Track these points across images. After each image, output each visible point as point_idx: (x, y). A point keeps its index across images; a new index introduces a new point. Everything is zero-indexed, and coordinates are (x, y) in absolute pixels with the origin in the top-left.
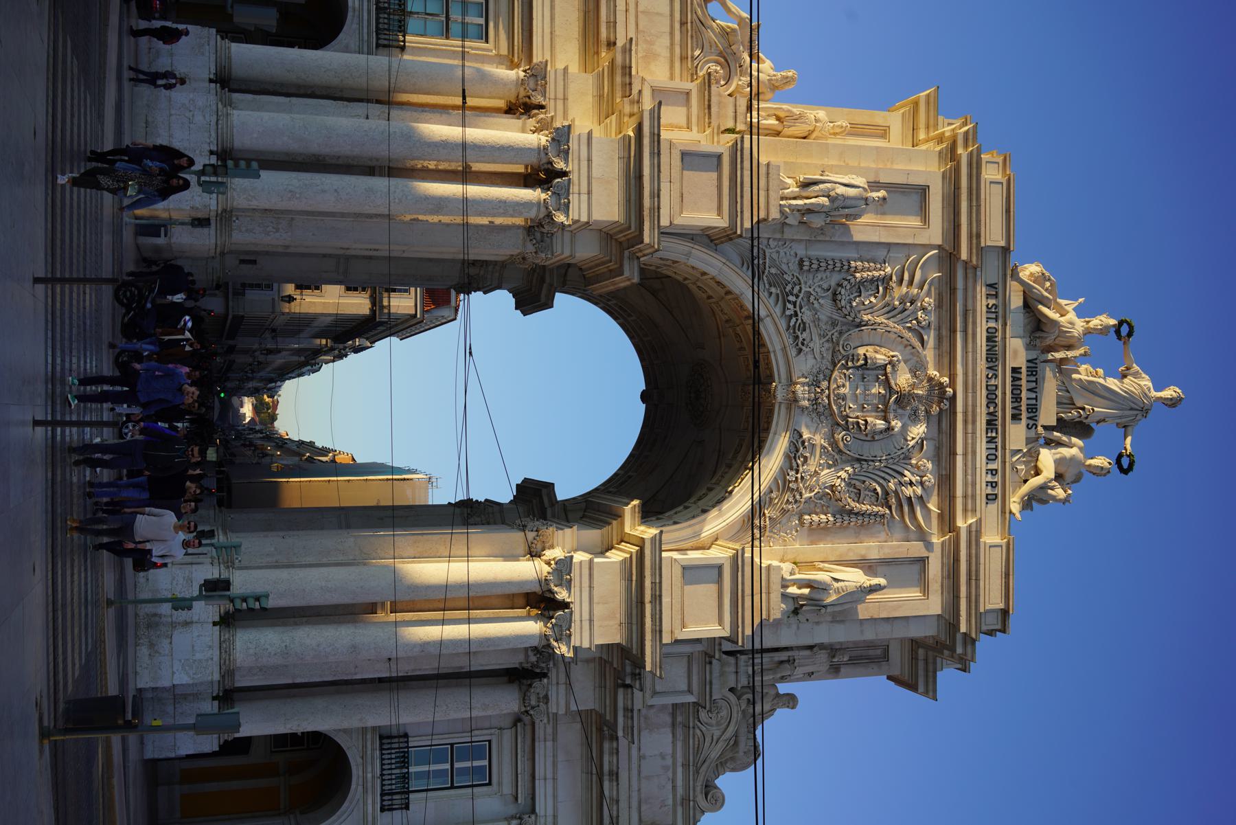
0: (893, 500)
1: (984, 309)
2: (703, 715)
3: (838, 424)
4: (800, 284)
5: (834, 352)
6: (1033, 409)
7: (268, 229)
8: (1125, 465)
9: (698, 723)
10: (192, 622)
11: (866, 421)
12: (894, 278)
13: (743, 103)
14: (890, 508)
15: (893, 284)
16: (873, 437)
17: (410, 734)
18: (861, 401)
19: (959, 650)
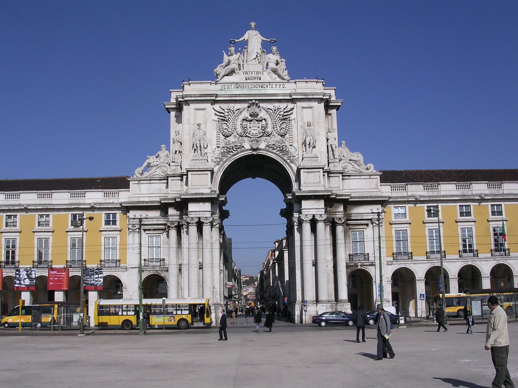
0: (285, 117)
1: (229, 89)
2: (346, 171)
3: (263, 135)
4: (224, 147)
5: (242, 137)
6: (257, 73)
7: (217, 294)
8: (274, 41)
9: (348, 172)
10: (317, 311)
11: (263, 127)
12: (221, 118)
13: (172, 164)
14: (287, 118)
15: (223, 118)
16: (267, 124)
17: (349, 253)
18: (256, 128)
19: (328, 97)
